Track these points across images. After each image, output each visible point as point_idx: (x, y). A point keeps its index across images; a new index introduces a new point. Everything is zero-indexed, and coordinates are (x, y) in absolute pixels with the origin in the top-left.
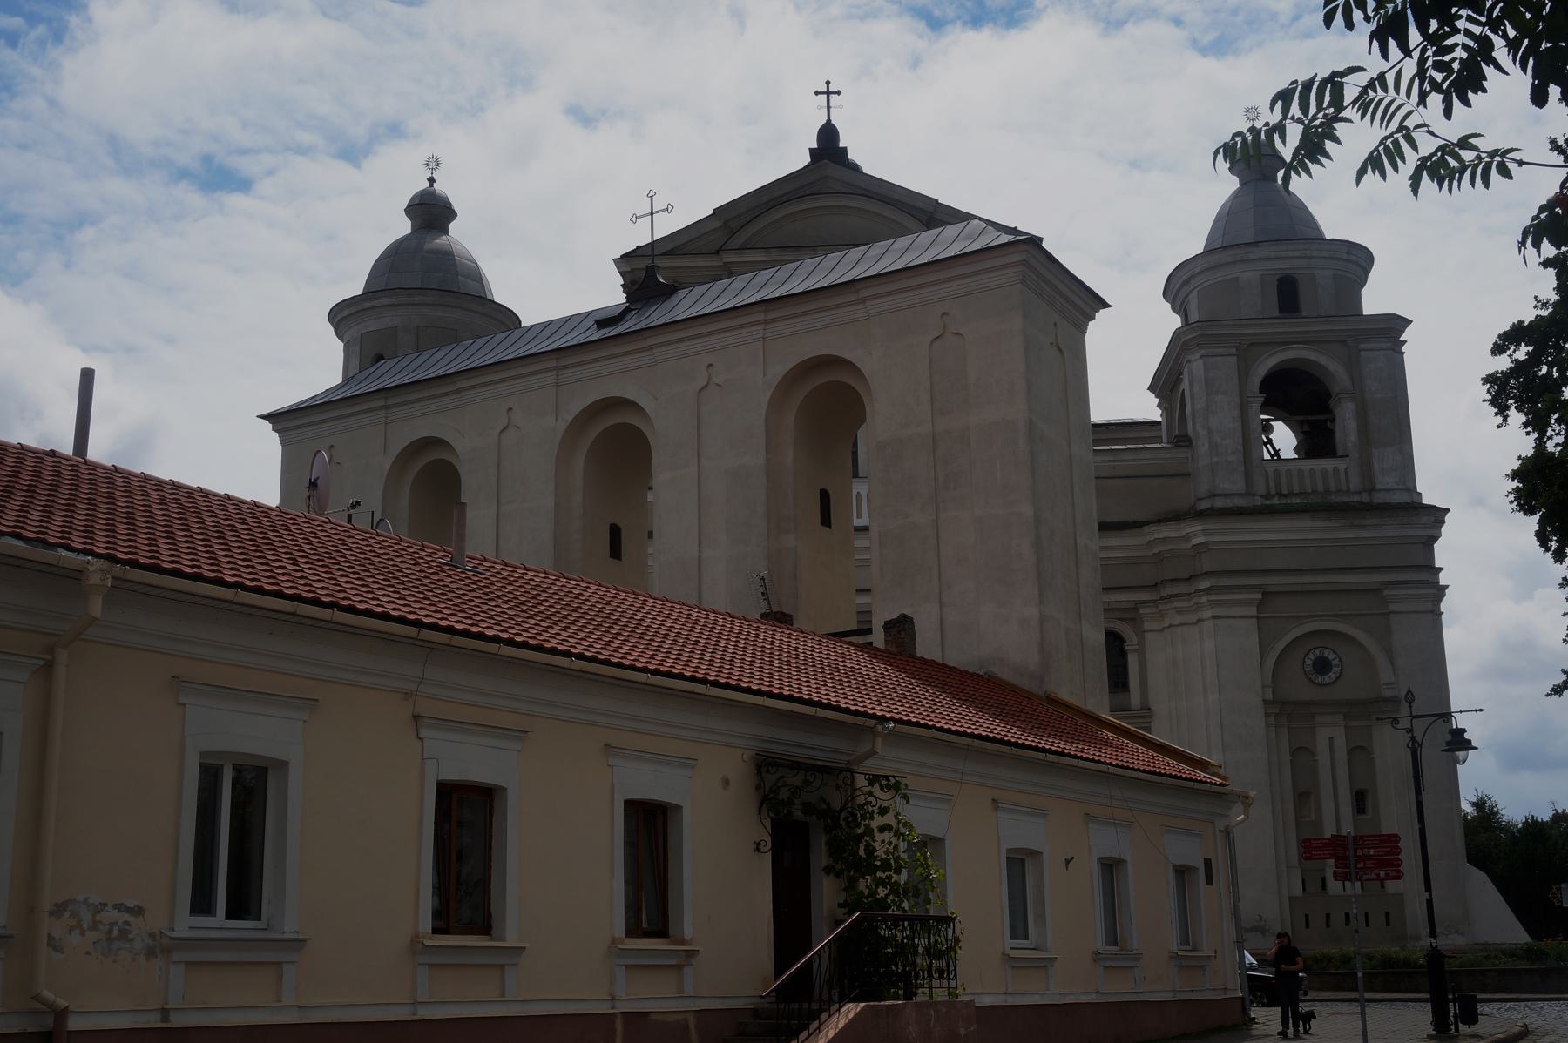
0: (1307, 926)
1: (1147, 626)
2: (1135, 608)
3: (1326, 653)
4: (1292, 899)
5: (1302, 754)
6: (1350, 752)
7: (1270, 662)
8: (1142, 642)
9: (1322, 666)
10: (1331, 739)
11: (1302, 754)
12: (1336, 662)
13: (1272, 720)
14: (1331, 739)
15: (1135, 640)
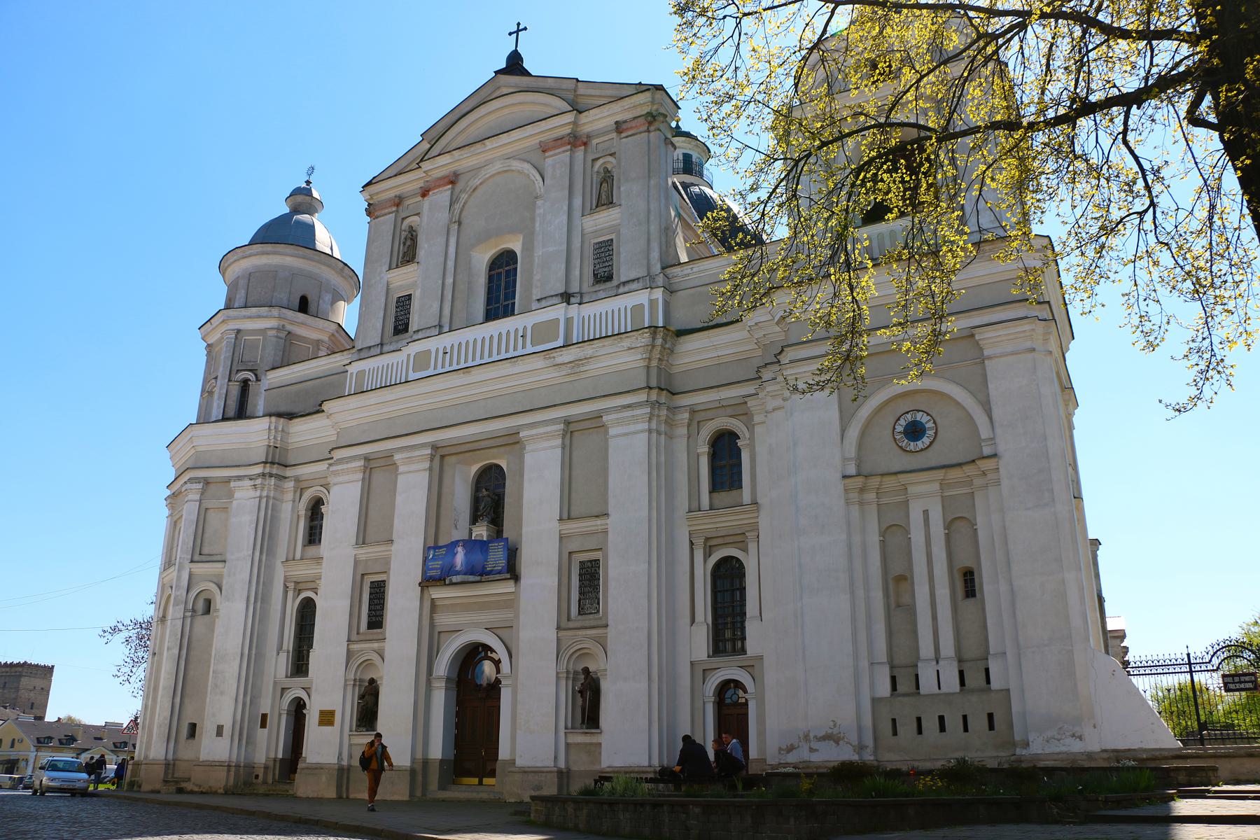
0: (895, 733)
1: (757, 419)
2: (744, 401)
3: (919, 416)
4: (875, 701)
5: (894, 533)
6: (948, 526)
7: (854, 432)
8: (752, 438)
9: (914, 431)
10: (926, 512)
11: (894, 533)
12: (931, 425)
13: (854, 496)
14: (926, 512)
15: (747, 436)
